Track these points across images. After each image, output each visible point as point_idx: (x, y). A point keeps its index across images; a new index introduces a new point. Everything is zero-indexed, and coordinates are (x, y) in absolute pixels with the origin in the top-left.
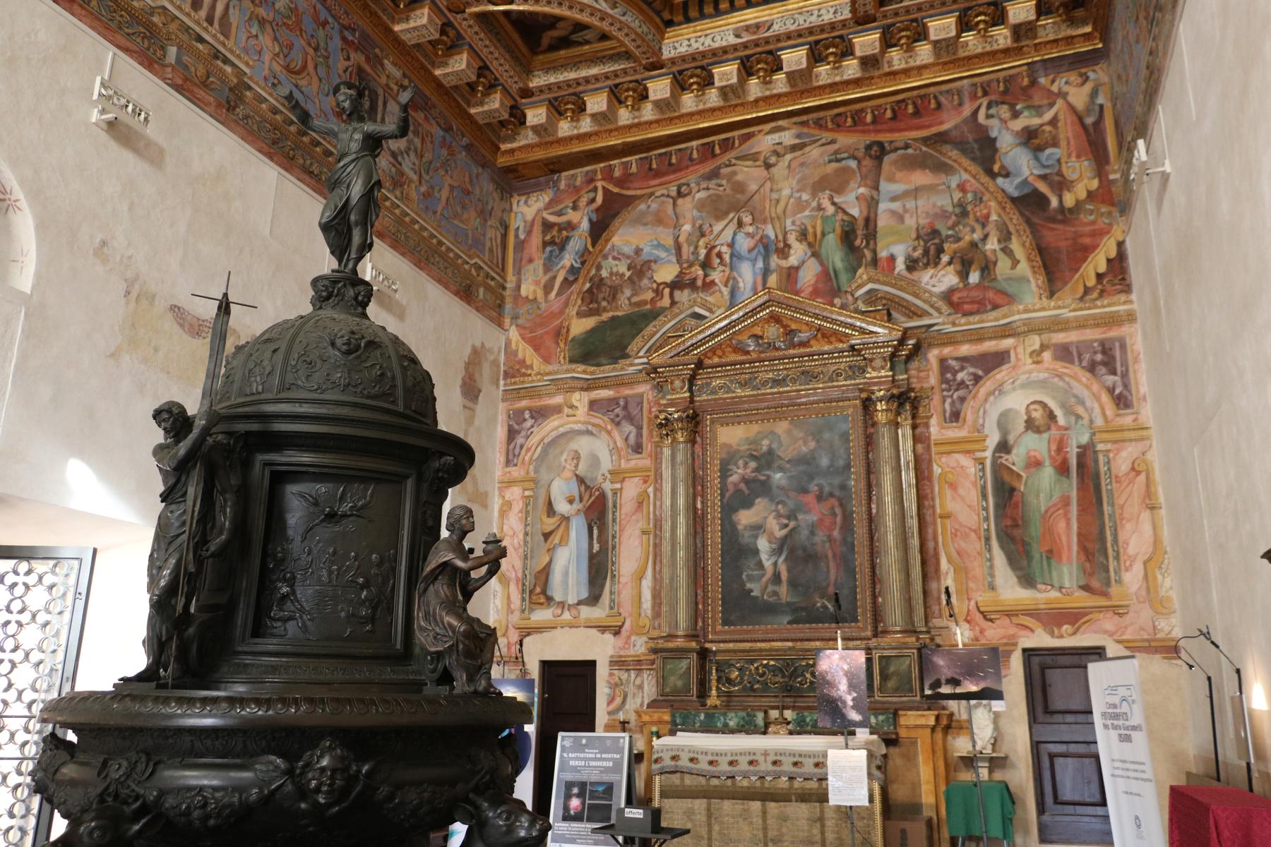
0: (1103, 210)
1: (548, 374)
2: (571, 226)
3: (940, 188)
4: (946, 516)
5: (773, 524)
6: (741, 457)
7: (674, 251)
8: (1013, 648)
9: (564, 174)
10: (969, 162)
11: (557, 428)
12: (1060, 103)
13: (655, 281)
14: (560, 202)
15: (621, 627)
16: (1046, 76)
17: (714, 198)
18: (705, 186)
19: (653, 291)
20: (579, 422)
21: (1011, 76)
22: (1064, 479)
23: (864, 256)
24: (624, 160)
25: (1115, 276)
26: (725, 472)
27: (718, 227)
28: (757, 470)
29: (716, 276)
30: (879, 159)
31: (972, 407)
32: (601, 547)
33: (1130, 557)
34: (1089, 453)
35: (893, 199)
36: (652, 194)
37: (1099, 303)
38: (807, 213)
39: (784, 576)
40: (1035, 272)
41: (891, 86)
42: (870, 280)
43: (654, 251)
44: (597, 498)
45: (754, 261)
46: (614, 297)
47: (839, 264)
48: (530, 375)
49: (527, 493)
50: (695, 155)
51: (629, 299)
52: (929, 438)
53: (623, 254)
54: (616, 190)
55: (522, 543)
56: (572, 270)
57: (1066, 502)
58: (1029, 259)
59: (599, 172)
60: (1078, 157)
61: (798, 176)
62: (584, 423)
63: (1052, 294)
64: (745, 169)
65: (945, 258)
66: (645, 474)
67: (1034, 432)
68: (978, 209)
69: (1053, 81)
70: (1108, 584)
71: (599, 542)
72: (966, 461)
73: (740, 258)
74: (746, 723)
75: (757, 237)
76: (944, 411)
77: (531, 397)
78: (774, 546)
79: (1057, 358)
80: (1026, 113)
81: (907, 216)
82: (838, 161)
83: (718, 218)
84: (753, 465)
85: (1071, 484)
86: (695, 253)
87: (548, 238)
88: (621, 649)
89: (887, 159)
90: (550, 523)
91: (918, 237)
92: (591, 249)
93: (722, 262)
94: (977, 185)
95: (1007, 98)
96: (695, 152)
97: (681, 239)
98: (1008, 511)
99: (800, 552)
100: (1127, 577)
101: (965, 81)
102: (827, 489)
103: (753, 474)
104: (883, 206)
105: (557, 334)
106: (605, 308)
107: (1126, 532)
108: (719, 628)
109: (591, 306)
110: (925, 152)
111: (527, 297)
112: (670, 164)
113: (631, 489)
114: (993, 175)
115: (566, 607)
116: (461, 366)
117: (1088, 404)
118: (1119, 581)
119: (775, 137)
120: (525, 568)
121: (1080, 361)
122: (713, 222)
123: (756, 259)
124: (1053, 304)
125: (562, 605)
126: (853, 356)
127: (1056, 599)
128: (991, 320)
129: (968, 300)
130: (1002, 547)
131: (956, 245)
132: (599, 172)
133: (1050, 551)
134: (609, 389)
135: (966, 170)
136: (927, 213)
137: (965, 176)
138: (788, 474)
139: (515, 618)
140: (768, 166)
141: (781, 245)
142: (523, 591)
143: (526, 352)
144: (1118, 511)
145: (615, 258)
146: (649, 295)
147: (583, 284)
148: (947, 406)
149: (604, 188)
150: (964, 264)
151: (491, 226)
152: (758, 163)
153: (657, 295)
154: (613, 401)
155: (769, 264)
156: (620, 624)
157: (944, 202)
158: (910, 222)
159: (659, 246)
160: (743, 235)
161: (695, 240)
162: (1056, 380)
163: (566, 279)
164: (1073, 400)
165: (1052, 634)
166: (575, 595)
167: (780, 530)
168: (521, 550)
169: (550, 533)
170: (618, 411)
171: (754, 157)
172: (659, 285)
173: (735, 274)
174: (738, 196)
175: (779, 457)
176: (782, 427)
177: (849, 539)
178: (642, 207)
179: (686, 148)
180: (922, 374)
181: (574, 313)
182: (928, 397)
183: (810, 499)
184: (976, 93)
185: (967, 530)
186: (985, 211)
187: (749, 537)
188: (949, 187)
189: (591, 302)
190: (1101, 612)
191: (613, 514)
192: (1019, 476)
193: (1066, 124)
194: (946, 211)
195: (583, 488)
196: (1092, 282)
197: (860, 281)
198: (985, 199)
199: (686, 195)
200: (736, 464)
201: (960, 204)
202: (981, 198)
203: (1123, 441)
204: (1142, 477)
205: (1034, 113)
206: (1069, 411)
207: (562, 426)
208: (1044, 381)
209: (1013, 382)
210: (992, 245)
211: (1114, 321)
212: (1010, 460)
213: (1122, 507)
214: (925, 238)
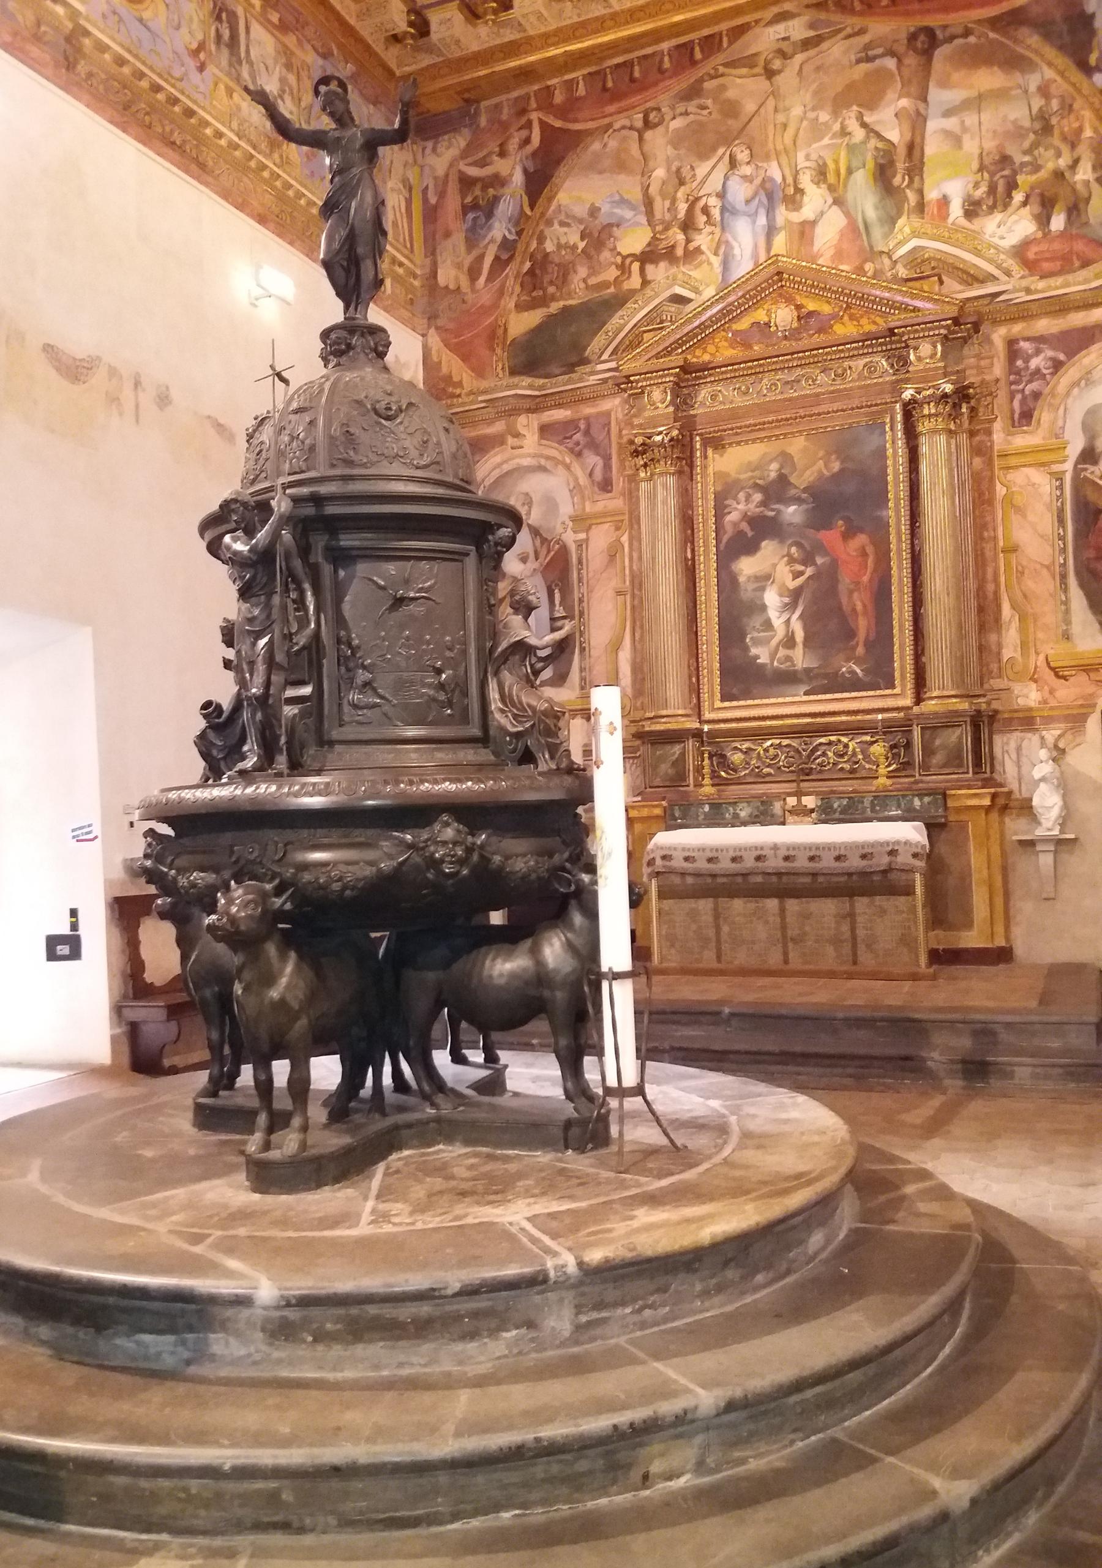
2: (498, 181)
3: (1014, 92)
5: (784, 573)
6: (742, 488)
8: (1090, 710)
9: (484, 104)
11: (499, 465)
13: (619, 254)
20: (529, 455)
23: (906, 198)
24: (567, 77)
26: (720, 512)
27: (702, 169)
28: (764, 504)
30: (927, 54)
35: (948, 113)
38: (826, 141)
42: (915, 234)
43: (616, 210)
45: (754, 216)
47: (871, 214)
48: (459, 396)
50: (667, 64)
51: (584, 280)
52: (992, 447)
53: (574, 217)
54: (558, 124)
56: (507, 245)
61: (814, 86)
62: (535, 456)
64: (738, 81)
65: (1018, 197)
66: (617, 518)
68: (1065, 122)
73: (734, 212)
74: (762, 813)
75: (758, 181)
76: (1012, 412)
78: (787, 600)
82: (869, 59)
83: (703, 156)
86: (673, 208)
87: (469, 199)
89: (940, 53)
91: (981, 169)
92: (529, 213)
93: (709, 222)
94: (1066, 86)
96: (666, 59)
97: (653, 190)
103: (758, 510)
104: (933, 125)
105: (493, 336)
109: (534, 294)
110: (991, 42)
111: (447, 287)
112: (632, 80)
113: (600, 538)
119: (779, 30)
123: (756, 212)
126: (891, 342)
129: (1047, 255)
130: (1082, 585)
135: (1050, 64)
136: (994, 132)
137: (1049, 73)
138: (804, 506)
140: (770, 74)
143: (452, 364)
145: (563, 224)
146: (612, 274)
147: (522, 263)
148: (1016, 404)
149: (540, 120)
150: (1046, 205)
151: (392, 190)
152: (757, 70)
153: (623, 273)
154: (570, 425)
157: (1018, 113)
158: (971, 146)
159: (623, 202)
160: (737, 178)
161: (671, 190)
163: (497, 258)
170: (578, 437)
171: (749, 61)
172: (624, 258)
173: (730, 239)
174: (730, 122)
176: (797, 446)
178: (596, 146)
179: (654, 54)
180: (983, 363)
181: (512, 305)
182: (991, 394)
185: (1038, 567)
186: (1076, 125)
187: (755, 590)
188: (1026, 91)
189: (534, 289)
194: (1021, 127)
195: (538, 542)
197: (900, 237)
198: (1076, 106)
199: (656, 125)
200: (735, 498)
202: (1071, 106)
207: (505, 462)
214: (992, 168)
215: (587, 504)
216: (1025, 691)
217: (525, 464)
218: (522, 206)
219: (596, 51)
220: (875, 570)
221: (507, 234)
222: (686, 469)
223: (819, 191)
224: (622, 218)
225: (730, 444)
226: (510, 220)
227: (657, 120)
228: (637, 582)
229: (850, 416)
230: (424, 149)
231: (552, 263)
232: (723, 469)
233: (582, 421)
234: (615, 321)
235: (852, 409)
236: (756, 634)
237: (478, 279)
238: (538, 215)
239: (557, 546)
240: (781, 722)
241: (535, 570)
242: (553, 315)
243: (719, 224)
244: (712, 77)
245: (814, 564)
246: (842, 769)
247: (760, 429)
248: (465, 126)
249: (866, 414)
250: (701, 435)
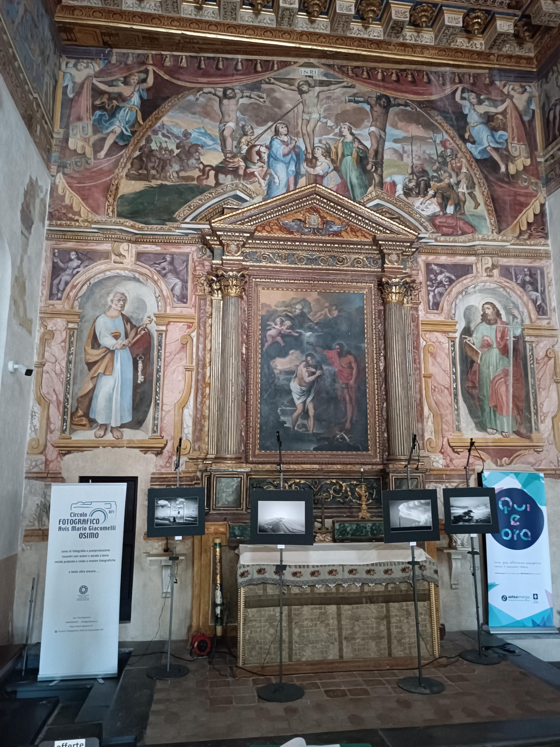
0: (533, 181)
1: (96, 223)
2: (120, 97)
4: (429, 376)
5: (303, 371)
7: (219, 142)
9: (115, 50)
10: (448, 127)
11: (104, 271)
12: (508, 101)
13: (202, 163)
14: (111, 74)
15: (163, 448)
16: (500, 81)
17: (256, 106)
18: (248, 94)
19: (200, 170)
21: (478, 74)
22: (504, 357)
25: (538, 226)
27: (258, 131)
29: (255, 169)
31: (448, 301)
32: (145, 379)
33: (544, 414)
34: (521, 341)
35: (396, 141)
36: (200, 89)
37: (528, 242)
38: (331, 136)
39: (311, 412)
40: (489, 214)
41: (401, 55)
42: (377, 197)
44: (142, 336)
45: (288, 164)
46: (163, 168)
47: (355, 181)
48: (77, 221)
49: (71, 325)
50: (240, 67)
51: (177, 173)
52: (418, 318)
53: (172, 134)
54: (166, 77)
55: (64, 370)
57: (506, 373)
58: (486, 204)
59: (150, 58)
60: (519, 141)
61: (325, 106)
62: (132, 271)
63: (500, 231)
64: (282, 89)
65: (431, 192)
67: (487, 324)
68: (453, 161)
69: (504, 86)
70: (531, 431)
71: (143, 373)
72: (443, 338)
75: (291, 146)
77: (78, 241)
78: (304, 388)
79: (502, 275)
80: (487, 103)
81: (405, 156)
83: (259, 124)
84: (288, 323)
85: (509, 362)
86: (238, 146)
88: (161, 466)
90: (94, 354)
91: (412, 173)
92: (141, 122)
93: (261, 159)
94: (454, 145)
95: (475, 89)
96: (240, 64)
97: (227, 133)
98: (470, 376)
99: (324, 395)
100: (542, 427)
101: (448, 69)
102: (346, 348)
104: (388, 145)
106: (154, 175)
107: (542, 396)
108: (257, 452)
109: (141, 172)
111: (75, 151)
112: (217, 68)
114: (465, 141)
115: (109, 429)
116: (22, 192)
117: (521, 309)
118: (537, 430)
119: (308, 71)
120: (67, 392)
121: (517, 279)
122: (254, 126)
124: (500, 238)
125: (105, 427)
127: (499, 439)
128: (461, 241)
130: (465, 401)
131: (439, 184)
132: (150, 58)
133: (496, 407)
134: (157, 245)
136: (419, 157)
137: (446, 137)
138: (316, 333)
139: (55, 437)
140: (301, 92)
141: (310, 156)
142: (65, 413)
144: (537, 383)
145: (164, 135)
146: (196, 173)
147: (134, 151)
149: (154, 72)
152: (293, 87)
153: (204, 175)
154: (161, 256)
155: (300, 169)
156: (163, 445)
160: (279, 141)
161: (239, 137)
162: (501, 290)
163: (115, 143)
164: (512, 305)
165: (496, 463)
166: (119, 419)
168: (63, 376)
169: (95, 363)
171: (290, 82)
172: (205, 166)
173: (273, 172)
174: (276, 110)
175: (309, 319)
176: (313, 297)
177: (362, 388)
178: (191, 98)
179: (232, 59)
181: (124, 174)
182: (417, 290)
183: (333, 354)
184: (454, 79)
185: (443, 388)
186: (459, 165)
187: (283, 380)
188: (435, 142)
189: (141, 169)
190: (526, 449)
191: (158, 352)
192: (477, 353)
193: (512, 117)
194: (433, 158)
195: (128, 327)
196: (524, 228)
197: (370, 196)
198: (459, 155)
199: (230, 98)
200: (274, 321)
201: (442, 155)
202: (456, 155)
203: (542, 336)
204: (553, 360)
205: (492, 104)
206: (509, 312)
207: (109, 270)
208: (493, 289)
209: (475, 287)
210: (462, 189)
211: (536, 255)
212: (472, 341)
213: (540, 381)
214: (418, 174)
215: (168, 308)
216: (437, 459)
217: (124, 274)
218: (136, 118)
219: (201, 42)
221: (124, 130)
223: (326, 161)
224: (205, 143)
226: (127, 123)
227: (231, 95)
228: (201, 363)
230: (67, 63)
231: (155, 156)
233: (168, 256)
234: (196, 201)
237: (100, 151)
238: (147, 126)
239: (143, 332)
241: (124, 345)
242: (152, 187)
243: (266, 163)
244: (267, 83)
248: (100, 59)
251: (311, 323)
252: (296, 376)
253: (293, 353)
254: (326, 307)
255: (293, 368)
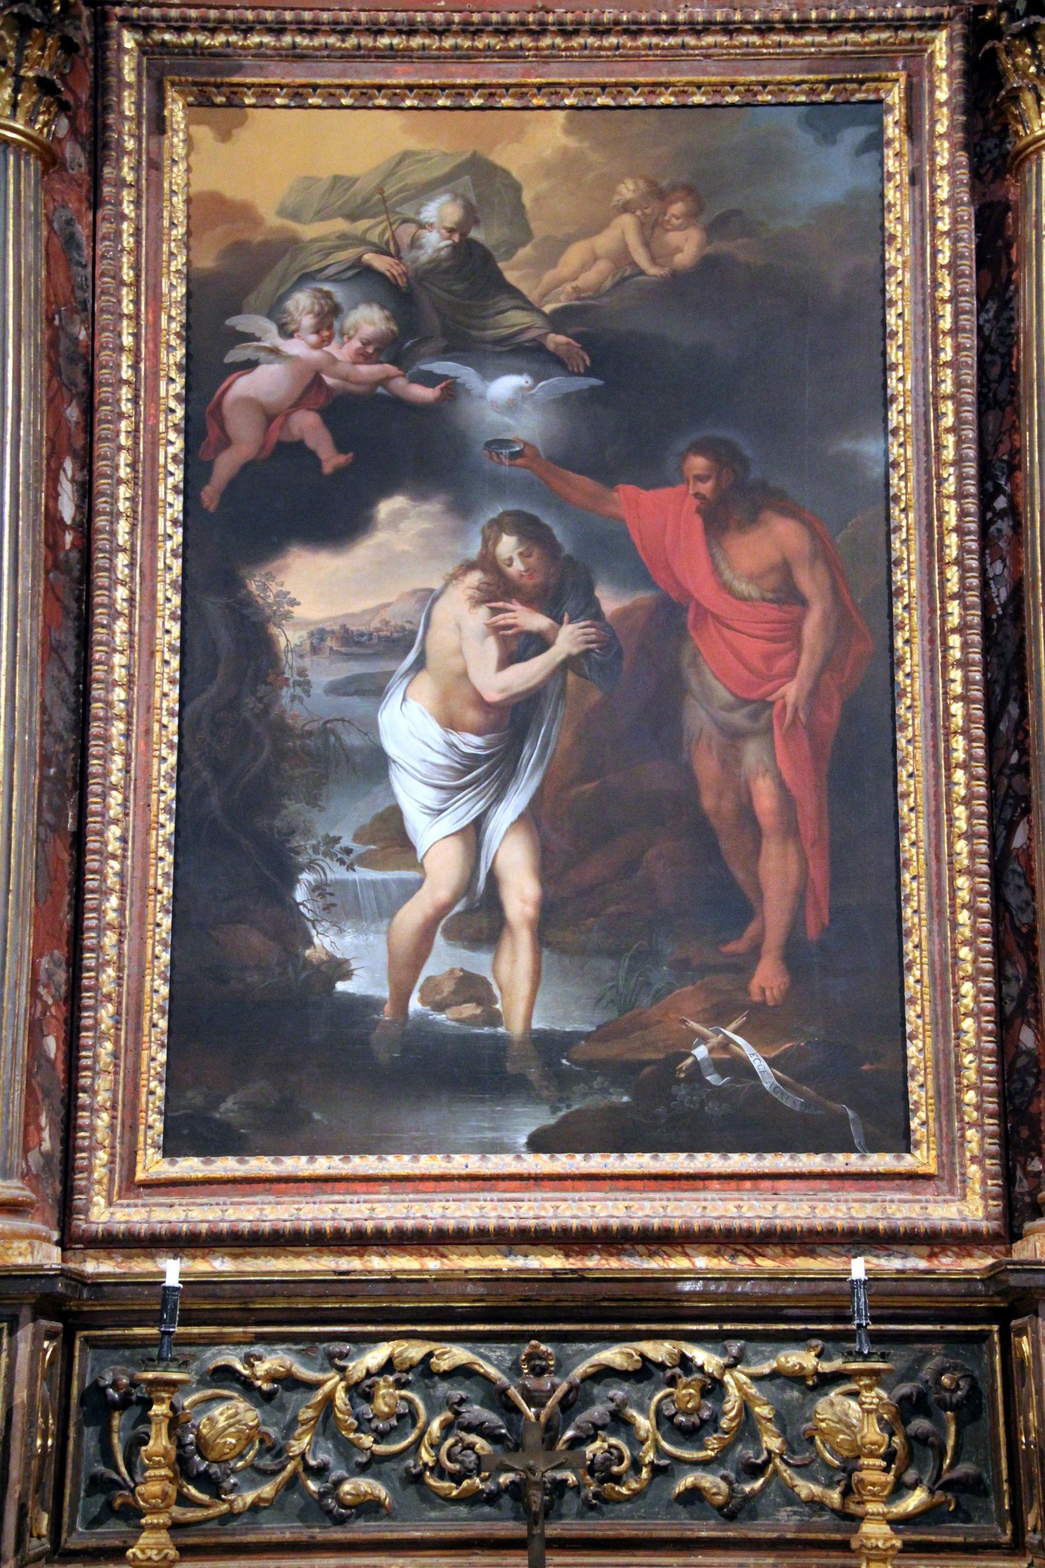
6: (306, 278)
78: (471, 743)
103: (366, 370)
138: (558, 383)
167: (509, 658)
175: (513, 292)
187: (336, 689)
200: (275, 311)
220: (828, 664)
222: (73, 153)
225: (265, 92)
229: (751, 55)
232: (233, 191)
235: (764, 28)
236: (336, 873)
240: (433, 1264)
245: (590, 610)
246: (694, 1496)
247: (392, 54)
249: (814, 61)
250: (143, 26)
251: (517, 318)
252: (420, 664)
253: (398, 516)
254: (626, 208)
255: (398, 615)
